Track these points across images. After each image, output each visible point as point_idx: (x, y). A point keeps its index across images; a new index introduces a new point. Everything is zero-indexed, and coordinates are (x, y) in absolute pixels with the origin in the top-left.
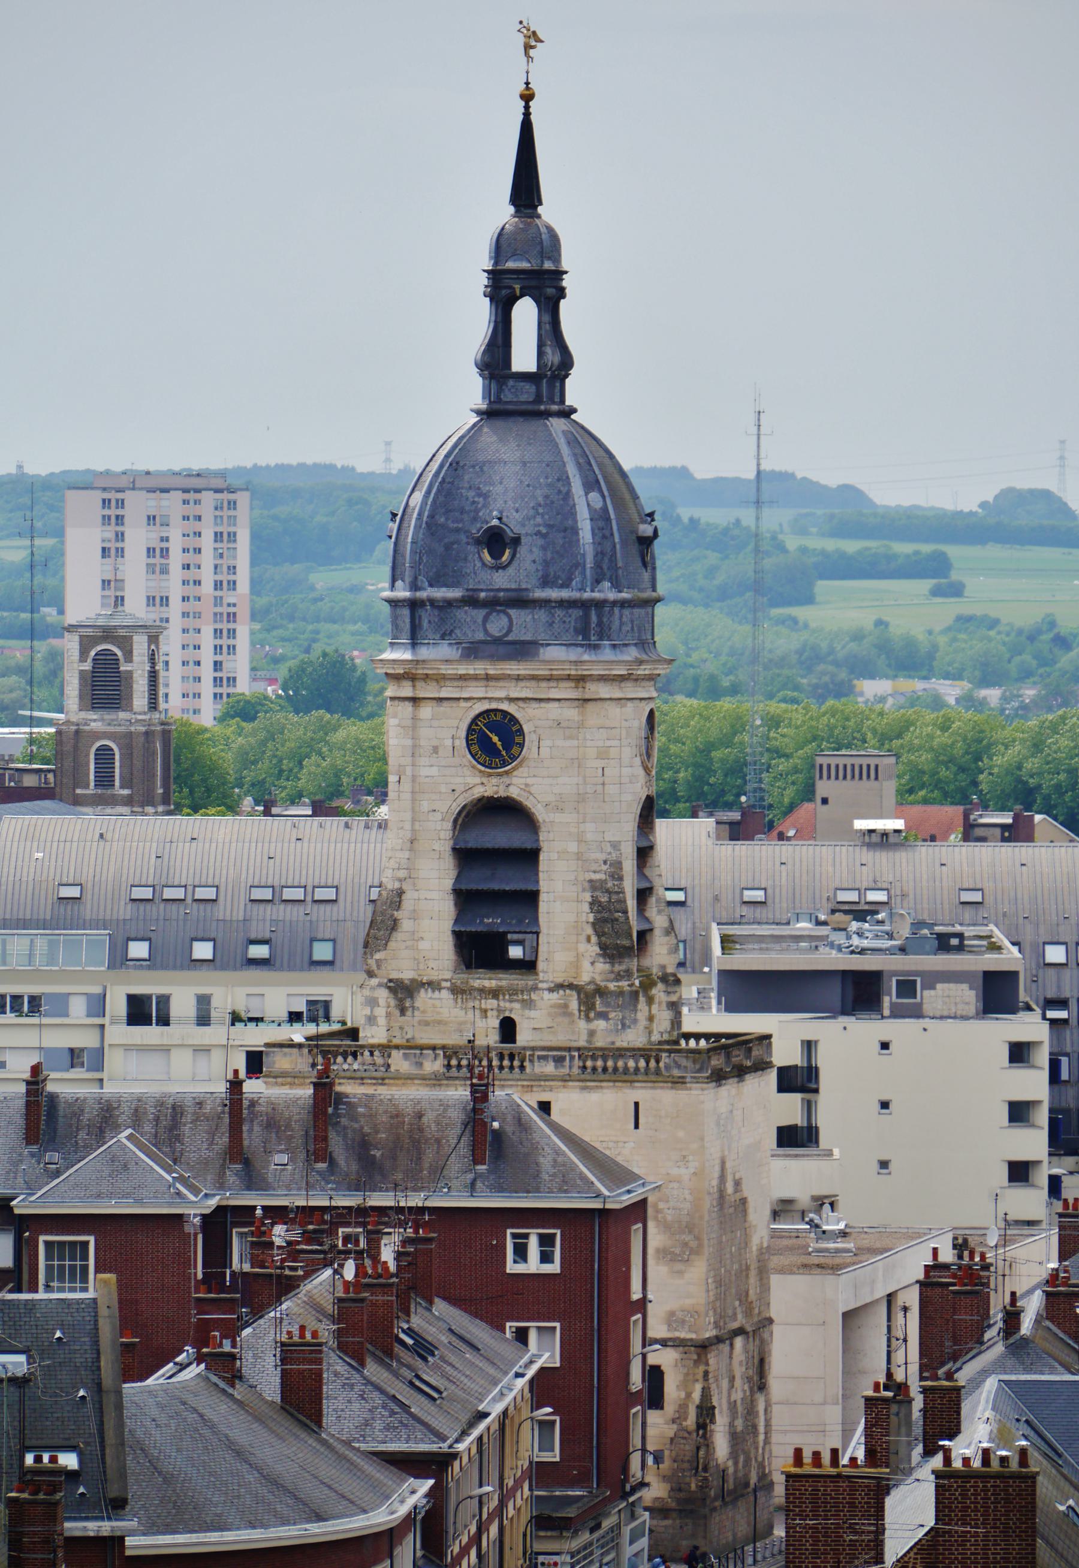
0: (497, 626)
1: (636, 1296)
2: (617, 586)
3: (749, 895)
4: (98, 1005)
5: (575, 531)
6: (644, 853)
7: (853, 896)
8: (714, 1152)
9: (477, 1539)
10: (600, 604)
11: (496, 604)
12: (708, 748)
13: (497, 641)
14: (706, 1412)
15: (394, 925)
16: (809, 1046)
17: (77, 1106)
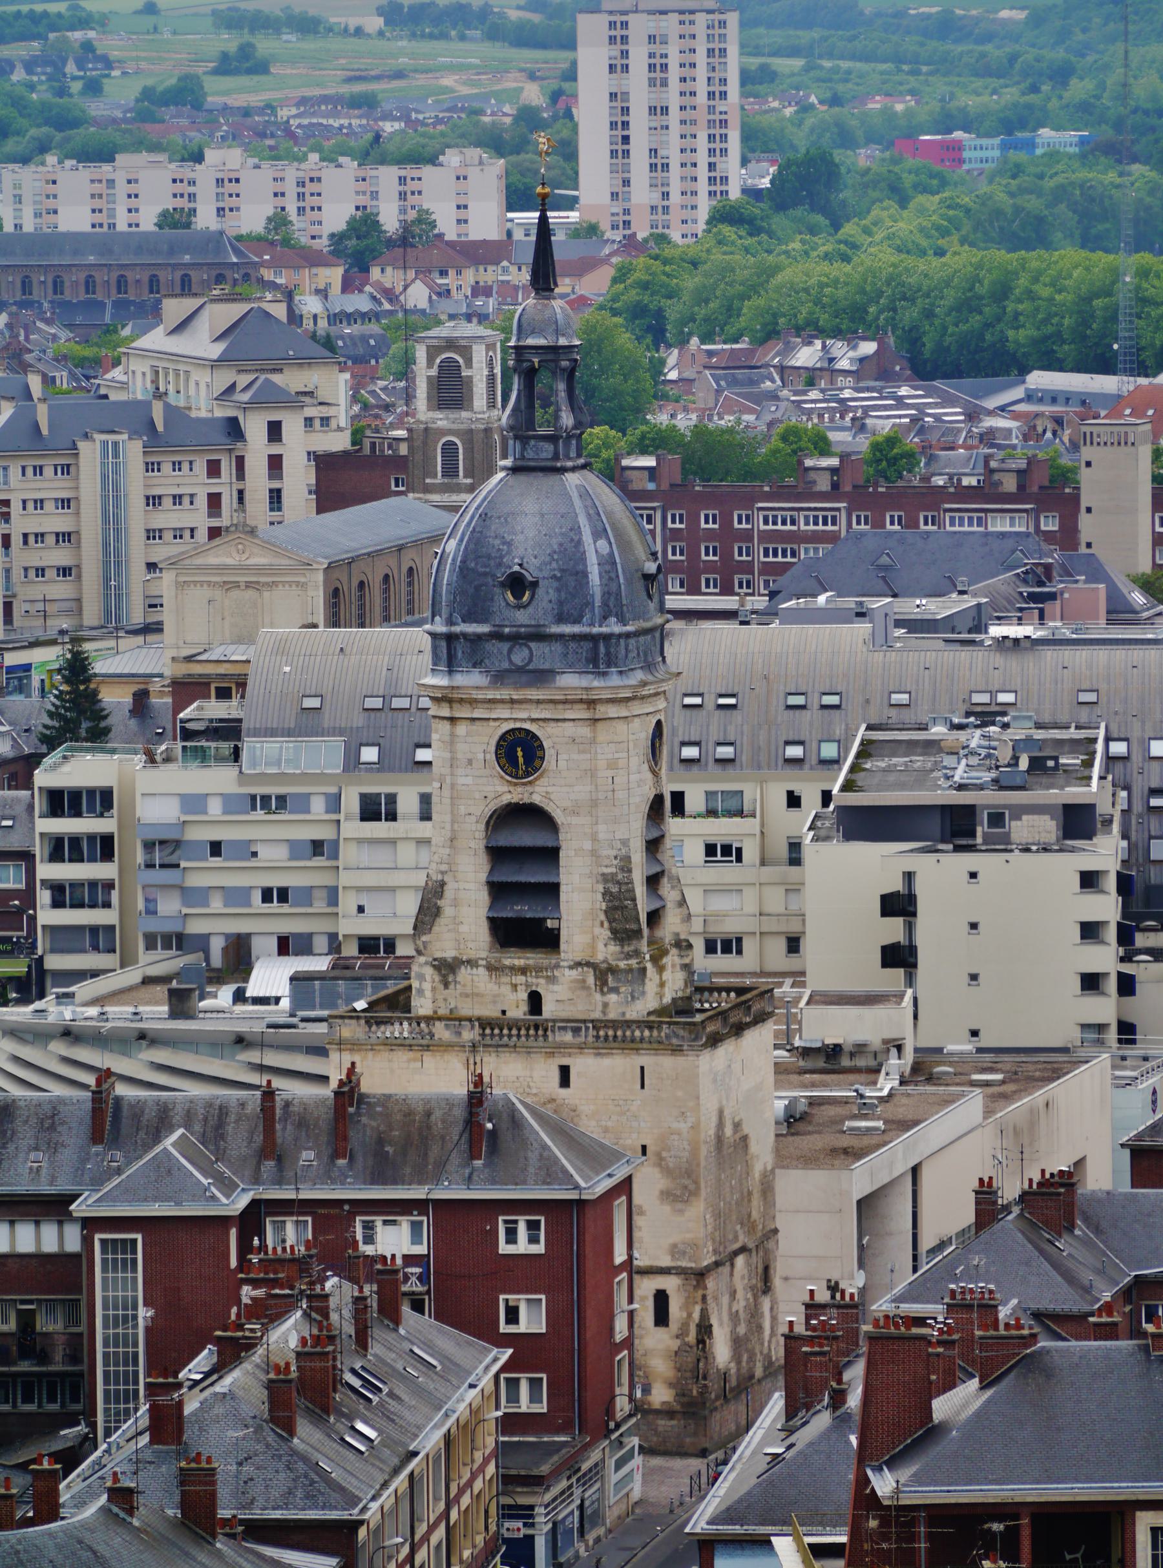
0: (519, 657)
1: (620, 1257)
2: (623, 621)
3: (896, 698)
4: (334, 803)
5: (585, 574)
6: (653, 846)
7: (984, 698)
8: (709, 1105)
9: (446, 1514)
10: (607, 638)
11: (516, 639)
12: (1088, 300)
13: (521, 670)
14: (705, 1329)
15: (437, 912)
16: (909, 876)
17: (138, 1107)
